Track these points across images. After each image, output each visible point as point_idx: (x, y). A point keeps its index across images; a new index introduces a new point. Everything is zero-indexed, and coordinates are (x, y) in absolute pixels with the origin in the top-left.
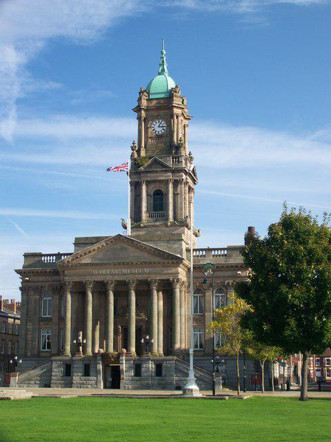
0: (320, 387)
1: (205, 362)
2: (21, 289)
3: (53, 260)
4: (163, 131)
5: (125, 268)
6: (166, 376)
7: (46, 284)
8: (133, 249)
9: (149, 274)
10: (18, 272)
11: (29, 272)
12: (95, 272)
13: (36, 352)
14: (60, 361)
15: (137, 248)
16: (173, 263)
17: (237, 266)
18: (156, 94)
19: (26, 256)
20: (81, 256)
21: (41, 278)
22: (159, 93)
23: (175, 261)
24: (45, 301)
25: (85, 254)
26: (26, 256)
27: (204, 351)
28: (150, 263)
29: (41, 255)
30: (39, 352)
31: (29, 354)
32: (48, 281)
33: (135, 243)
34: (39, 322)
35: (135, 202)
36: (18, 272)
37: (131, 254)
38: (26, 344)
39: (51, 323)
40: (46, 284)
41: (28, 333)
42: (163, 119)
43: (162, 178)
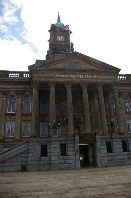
3: (17, 76)
5: (82, 74)
7: (12, 90)
9: (97, 79)
12: (58, 76)
16: (113, 72)
21: (8, 86)
22: (60, 26)
24: (10, 102)
25: (51, 63)
28: (99, 71)
29: (9, 72)
30: (4, 138)
32: (14, 88)
34: (5, 116)
40: (12, 90)
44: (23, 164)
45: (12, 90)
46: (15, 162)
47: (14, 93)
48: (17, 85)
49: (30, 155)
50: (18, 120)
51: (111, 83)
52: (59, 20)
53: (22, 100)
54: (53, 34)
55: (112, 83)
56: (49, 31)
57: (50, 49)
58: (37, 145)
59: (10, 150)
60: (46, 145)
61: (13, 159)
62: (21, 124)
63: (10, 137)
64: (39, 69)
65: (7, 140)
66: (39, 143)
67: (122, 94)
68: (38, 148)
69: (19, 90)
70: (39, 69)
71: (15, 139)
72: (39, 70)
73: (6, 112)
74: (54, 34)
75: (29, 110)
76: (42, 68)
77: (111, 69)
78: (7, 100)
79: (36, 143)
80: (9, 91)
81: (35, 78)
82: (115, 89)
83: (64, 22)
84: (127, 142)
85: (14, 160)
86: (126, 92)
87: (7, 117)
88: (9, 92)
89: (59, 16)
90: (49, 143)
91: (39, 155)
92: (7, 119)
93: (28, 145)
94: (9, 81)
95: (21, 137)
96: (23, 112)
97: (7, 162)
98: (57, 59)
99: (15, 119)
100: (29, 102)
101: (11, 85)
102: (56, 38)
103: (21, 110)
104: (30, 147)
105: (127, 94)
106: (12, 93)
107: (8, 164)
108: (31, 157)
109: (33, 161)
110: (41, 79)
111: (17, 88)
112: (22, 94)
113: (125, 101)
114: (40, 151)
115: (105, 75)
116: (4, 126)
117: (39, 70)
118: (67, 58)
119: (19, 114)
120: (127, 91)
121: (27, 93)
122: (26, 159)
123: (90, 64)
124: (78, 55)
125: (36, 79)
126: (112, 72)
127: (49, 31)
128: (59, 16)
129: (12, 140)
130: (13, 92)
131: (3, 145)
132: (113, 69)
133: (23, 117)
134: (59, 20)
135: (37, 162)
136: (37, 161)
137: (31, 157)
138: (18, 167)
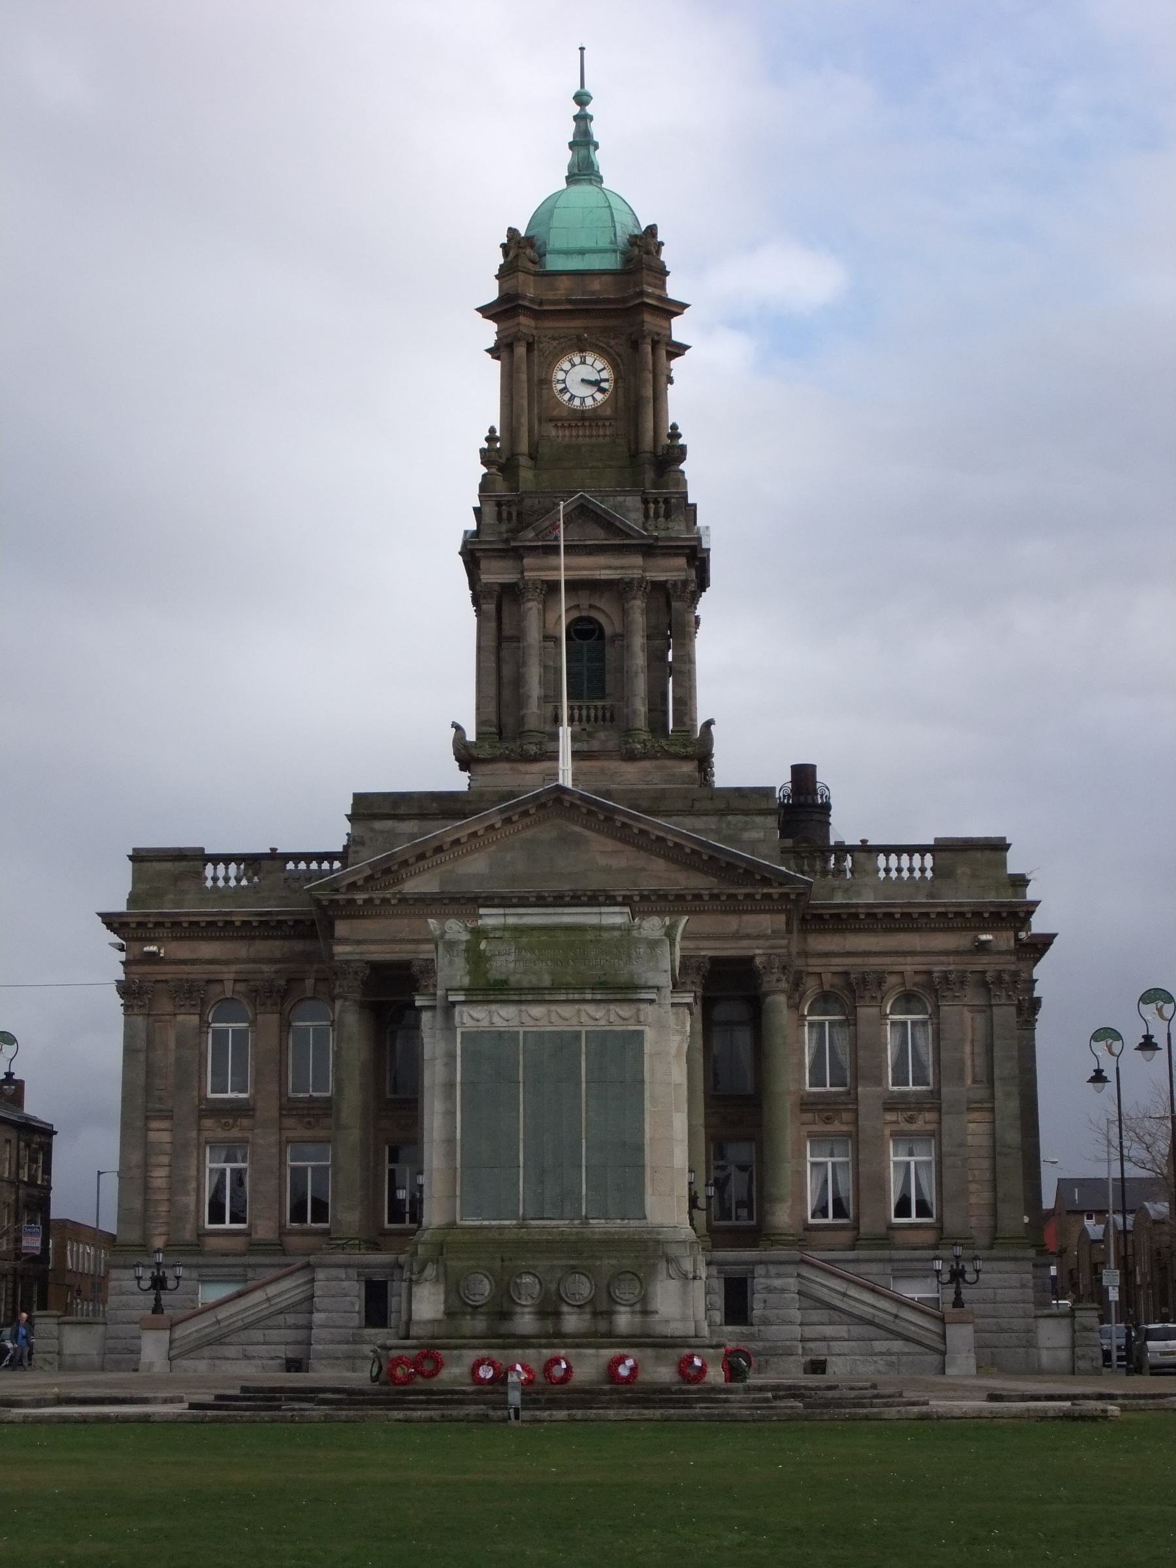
0: (1074, 1358)
1: (864, 1268)
2: (124, 989)
4: (599, 396)
6: (766, 1322)
8: (610, 845)
10: (111, 921)
11: (158, 924)
13: (188, 1235)
14: (347, 1266)
15: (623, 840)
17: (977, 914)
18: (568, 253)
19: (139, 857)
20: (405, 863)
21: (208, 950)
23: (774, 891)
24: (220, 1036)
25: (421, 857)
26: (139, 857)
27: (857, 1228)
28: (680, 897)
31: (159, 1242)
32: (236, 961)
33: (620, 819)
34: (200, 1117)
35: (499, 661)
36: (111, 921)
37: (602, 861)
38: (146, 1202)
39: (245, 1122)
40: (228, 973)
41: (154, 1160)
42: (603, 352)
43: (606, 574)
44: (291, 1352)
45: (224, 968)
46: (258, 1344)
47: (240, 987)
48: (253, 938)
49: (318, 1317)
50: (266, 1139)
51: (752, 958)
52: (583, 170)
53: (285, 1026)
54: (521, 350)
55: (758, 961)
56: (497, 277)
57: (490, 512)
58: (348, 1279)
59: (240, 1295)
60: (386, 1282)
61: (252, 1332)
62: (282, 1163)
63: (228, 1225)
64: (360, 897)
65: (212, 1243)
66: (353, 1273)
67: (880, 983)
68: (355, 1293)
69: (265, 968)
70: (360, 897)
71: (255, 1237)
72: (360, 902)
73: (203, 1098)
74: (530, 347)
75: (320, 1084)
76: (377, 895)
77: (758, 877)
78: (204, 1024)
79: (341, 1273)
80: (212, 977)
81: (345, 941)
82: (774, 992)
83: (640, 187)
84: (749, 1281)
85: (257, 1335)
86: (909, 966)
87: (208, 1123)
88: (209, 982)
89: (582, 99)
90: (397, 1272)
91: (356, 1319)
92: (206, 1134)
93: (313, 1280)
94: (210, 923)
95: (282, 1231)
96: (291, 1095)
97: (230, 1344)
98: (456, 836)
99: (248, 1135)
100: (321, 1035)
101: (219, 938)
102: (546, 382)
103: (282, 1083)
104: (319, 1288)
105: (918, 978)
106: (229, 986)
107: (231, 1351)
108: (321, 1326)
109: (332, 1342)
110: (373, 948)
111: (254, 961)
112: (278, 995)
113: (904, 1024)
114: (359, 1305)
115: (725, 912)
116: (193, 1172)
117: (360, 902)
118: (508, 821)
119: (268, 1109)
120: (918, 959)
121: (309, 983)
122: (301, 1334)
123: (639, 847)
124: (572, 804)
125: (348, 949)
126: (758, 897)
127: (497, 277)
128: (582, 99)
129: (239, 1243)
130: (235, 981)
131: (198, 1266)
132: (766, 882)
133: (289, 1122)
134: (583, 170)
135: (346, 1346)
136: (347, 1343)
137: (321, 1326)
138: (271, 1362)
